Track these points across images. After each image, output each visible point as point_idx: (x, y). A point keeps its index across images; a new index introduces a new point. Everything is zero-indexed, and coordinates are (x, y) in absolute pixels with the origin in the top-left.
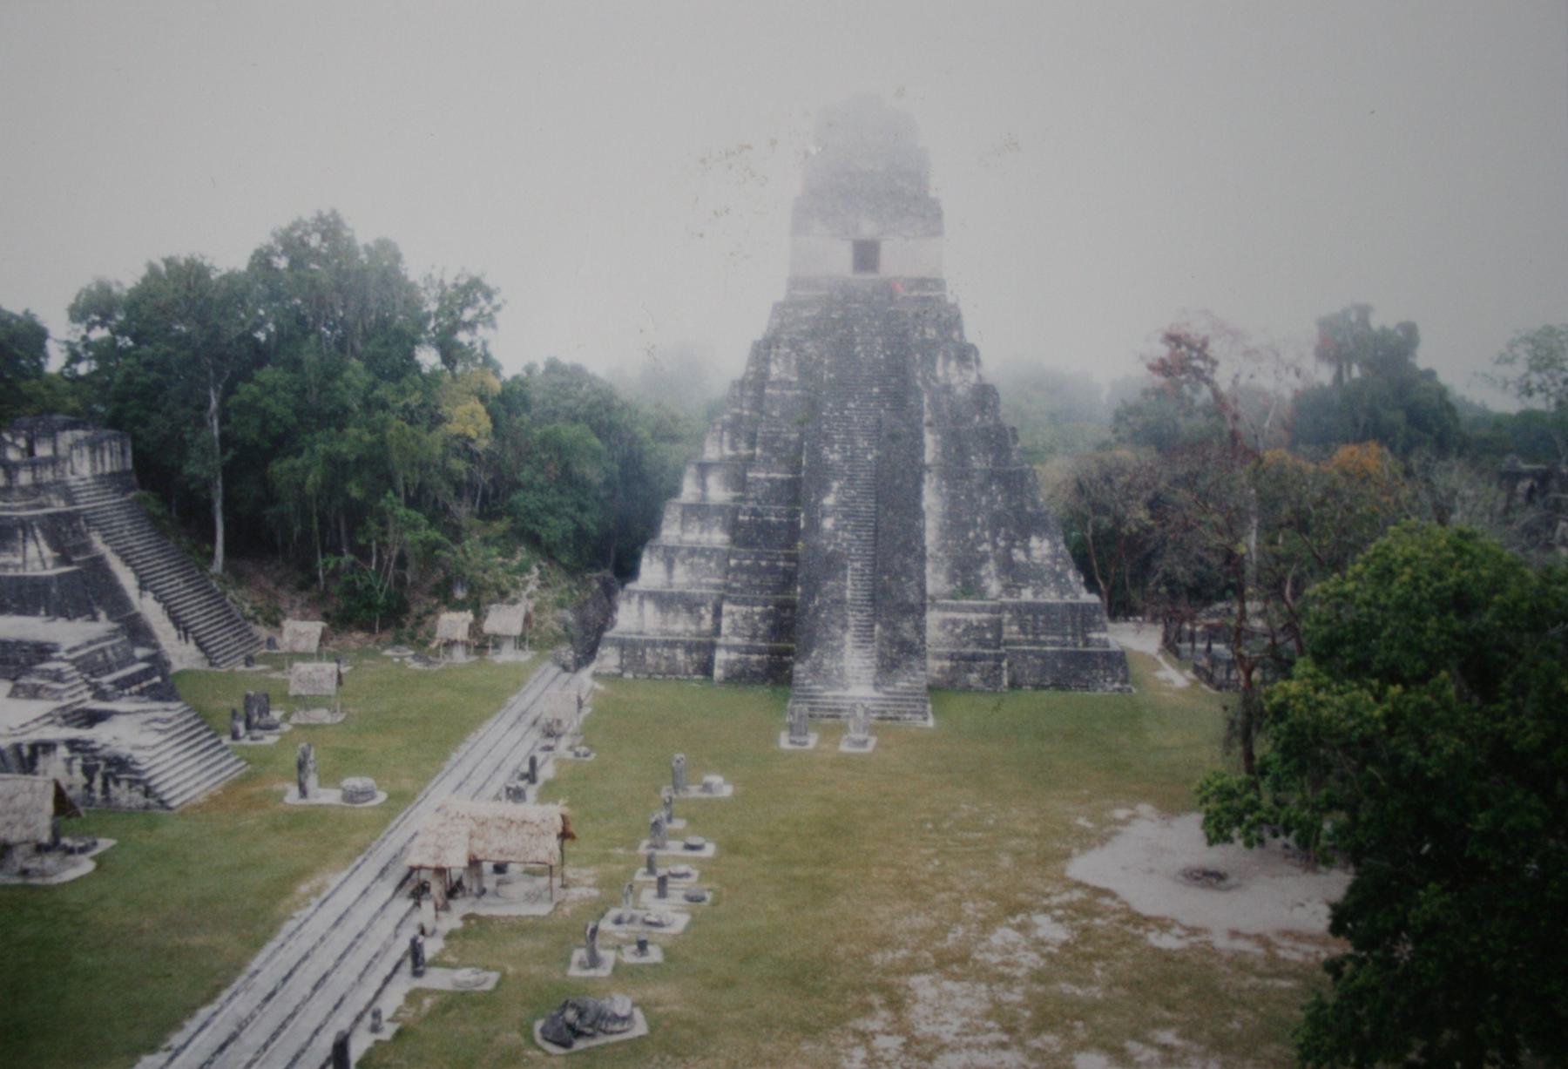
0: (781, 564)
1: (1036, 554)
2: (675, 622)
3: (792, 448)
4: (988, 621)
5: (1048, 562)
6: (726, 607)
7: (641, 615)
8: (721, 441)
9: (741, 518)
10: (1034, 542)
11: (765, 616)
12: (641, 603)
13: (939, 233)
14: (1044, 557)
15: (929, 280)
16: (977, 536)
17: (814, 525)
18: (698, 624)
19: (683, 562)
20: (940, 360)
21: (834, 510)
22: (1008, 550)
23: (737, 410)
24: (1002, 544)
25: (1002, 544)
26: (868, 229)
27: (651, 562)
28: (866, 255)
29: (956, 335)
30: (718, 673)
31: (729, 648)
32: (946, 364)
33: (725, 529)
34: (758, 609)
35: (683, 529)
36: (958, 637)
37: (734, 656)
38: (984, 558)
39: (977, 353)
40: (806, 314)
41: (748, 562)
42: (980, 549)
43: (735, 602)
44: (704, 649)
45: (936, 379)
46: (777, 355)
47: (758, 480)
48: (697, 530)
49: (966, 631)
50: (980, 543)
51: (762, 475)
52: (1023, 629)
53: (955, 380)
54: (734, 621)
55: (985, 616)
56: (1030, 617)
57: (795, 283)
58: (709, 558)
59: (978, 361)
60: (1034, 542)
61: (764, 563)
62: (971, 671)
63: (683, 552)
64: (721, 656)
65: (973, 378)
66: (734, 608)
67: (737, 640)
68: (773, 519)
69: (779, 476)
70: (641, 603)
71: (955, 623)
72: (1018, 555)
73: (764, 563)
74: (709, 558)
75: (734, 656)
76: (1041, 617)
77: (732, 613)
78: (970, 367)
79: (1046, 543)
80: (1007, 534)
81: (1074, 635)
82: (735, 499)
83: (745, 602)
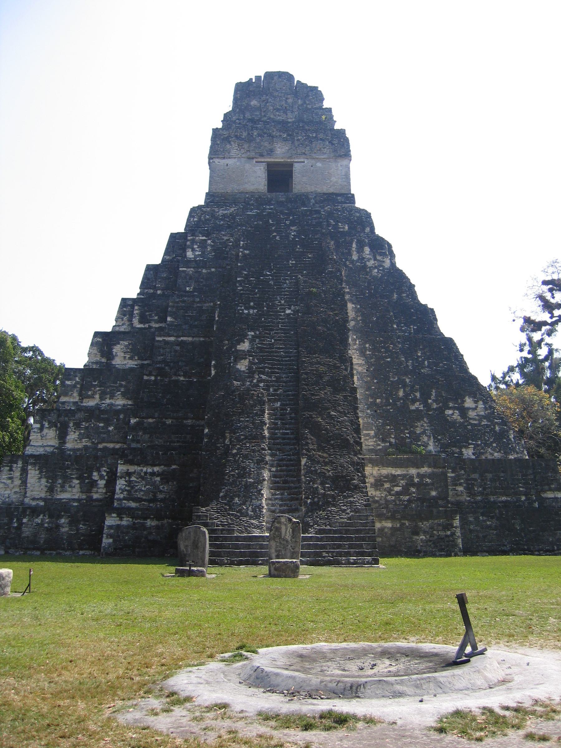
0: (189, 422)
1: (472, 414)
2: (63, 491)
3: (204, 317)
4: (430, 476)
5: (485, 422)
6: (121, 468)
7: (24, 482)
8: (131, 315)
9: (145, 378)
10: (469, 402)
11: (166, 477)
12: (24, 471)
13: (347, 155)
14: (481, 418)
15: (337, 195)
16: (406, 395)
17: (226, 372)
18: (89, 491)
19: (77, 426)
20: (354, 245)
21: (248, 353)
22: (441, 411)
23: (152, 291)
24: (435, 406)
25: (435, 406)
26: (281, 152)
27: (41, 429)
28: (280, 177)
29: (368, 230)
30: (106, 541)
31: (121, 512)
32: (360, 249)
33: (124, 395)
34: (156, 469)
35: (82, 396)
36: (398, 494)
37: (126, 521)
38: (418, 416)
39: (390, 246)
40: (221, 212)
41: (150, 420)
42: (413, 408)
43: (131, 463)
44: (92, 513)
45: (352, 262)
46: (193, 242)
47: (166, 343)
48: (97, 396)
49: (405, 491)
50: (414, 401)
51: (172, 339)
52: (469, 489)
53: (371, 263)
54: (129, 483)
55: (425, 470)
56: (476, 476)
57: (212, 197)
58: (108, 422)
59: (392, 255)
60: (469, 402)
61: (169, 422)
62: (416, 532)
63: (79, 415)
64: (111, 521)
65: (387, 264)
66: (132, 468)
67: (133, 505)
68: (182, 378)
69: (190, 339)
70: (24, 471)
71: (393, 479)
72: (453, 414)
73: (169, 422)
74: (108, 422)
75: (126, 521)
76: (489, 476)
77: (128, 474)
78: (384, 255)
79: (481, 405)
80: (438, 395)
81: (526, 494)
82: (142, 366)
83: (143, 462)
